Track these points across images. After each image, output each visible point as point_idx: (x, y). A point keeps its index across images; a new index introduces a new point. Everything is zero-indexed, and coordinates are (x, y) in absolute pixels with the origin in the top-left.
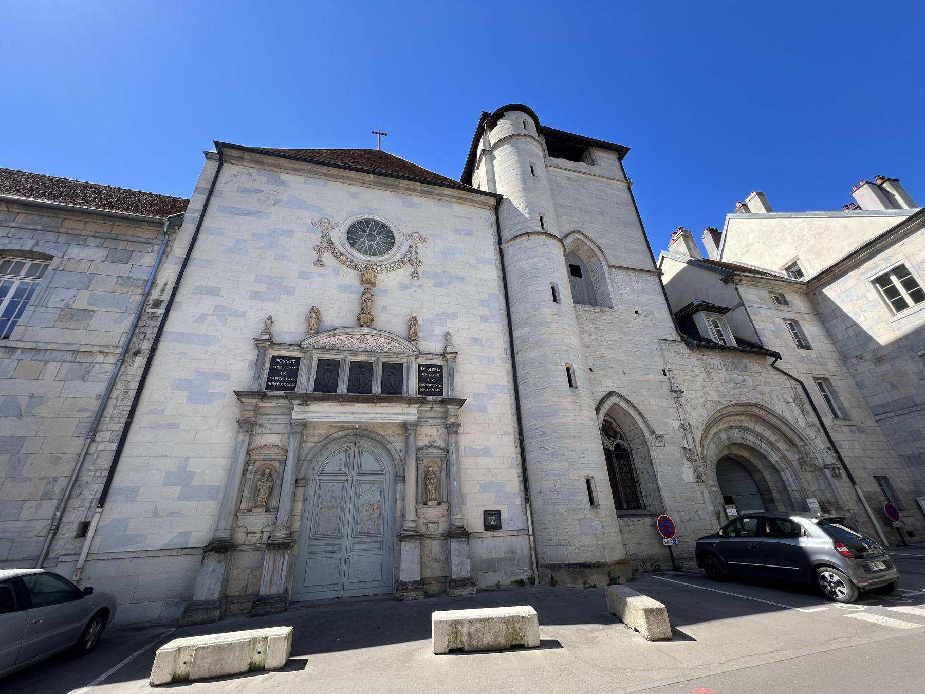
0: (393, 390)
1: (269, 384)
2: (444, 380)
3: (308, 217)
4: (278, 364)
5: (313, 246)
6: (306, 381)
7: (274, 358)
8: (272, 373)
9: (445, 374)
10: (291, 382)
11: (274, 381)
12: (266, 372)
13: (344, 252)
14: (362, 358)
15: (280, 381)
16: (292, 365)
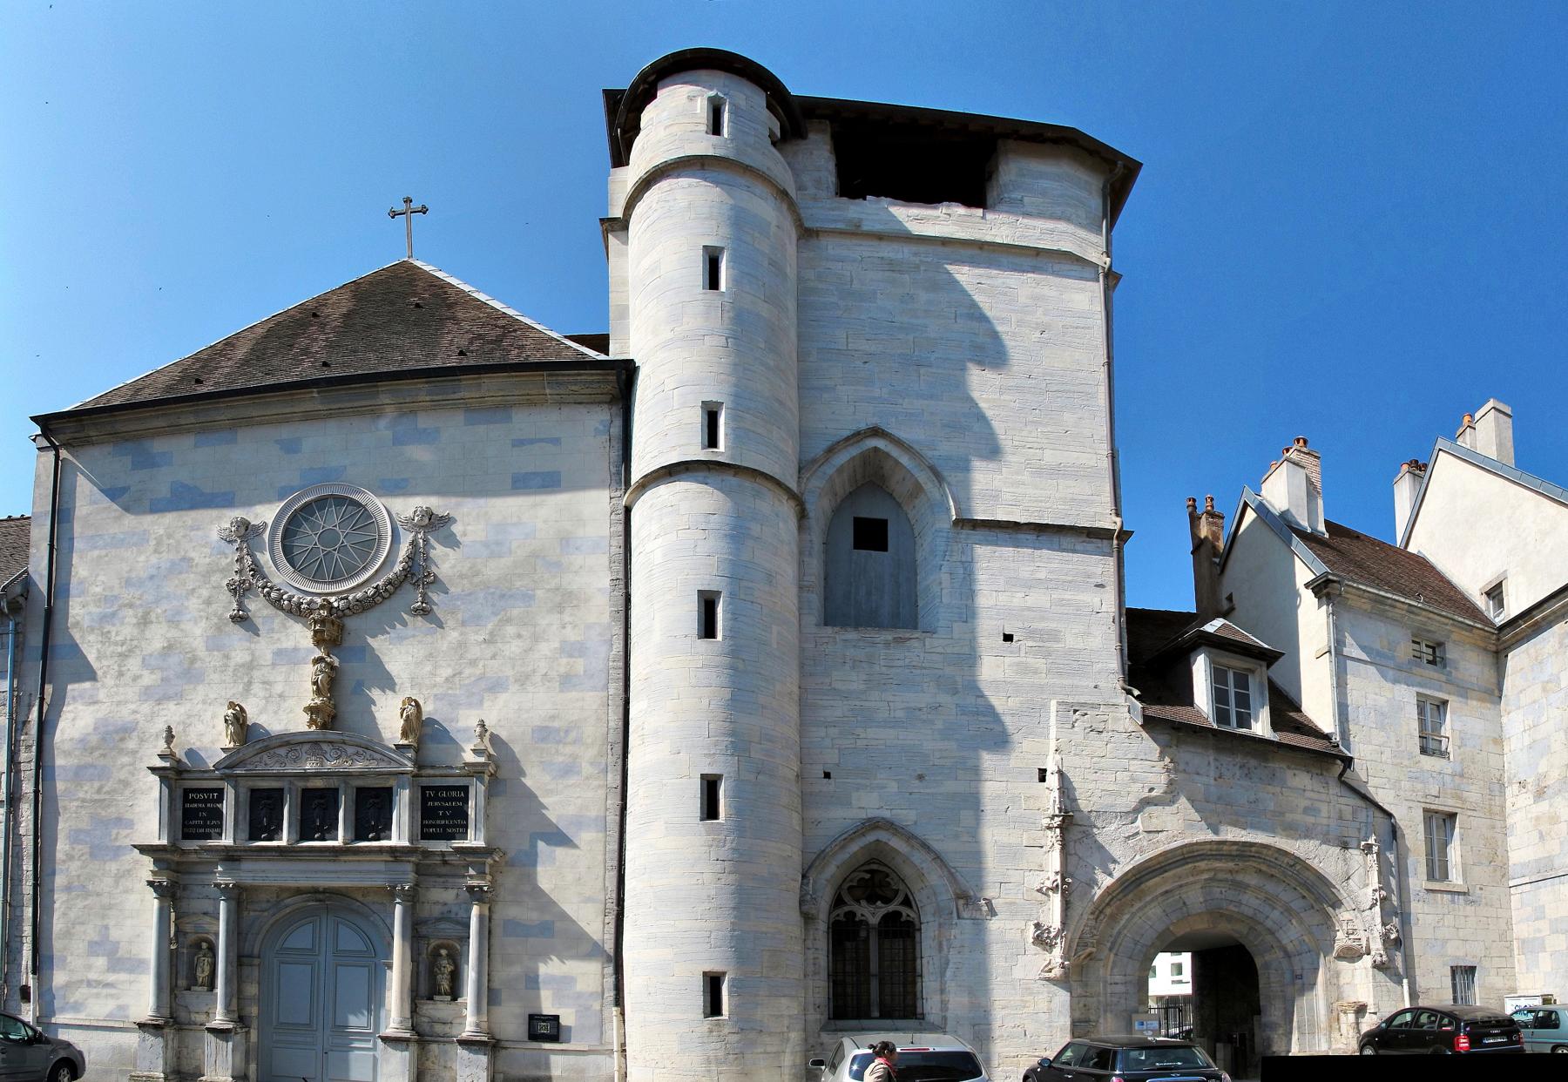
4: (193, 801)
7: (187, 792)
8: (188, 815)
12: (180, 813)
14: (318, 783)
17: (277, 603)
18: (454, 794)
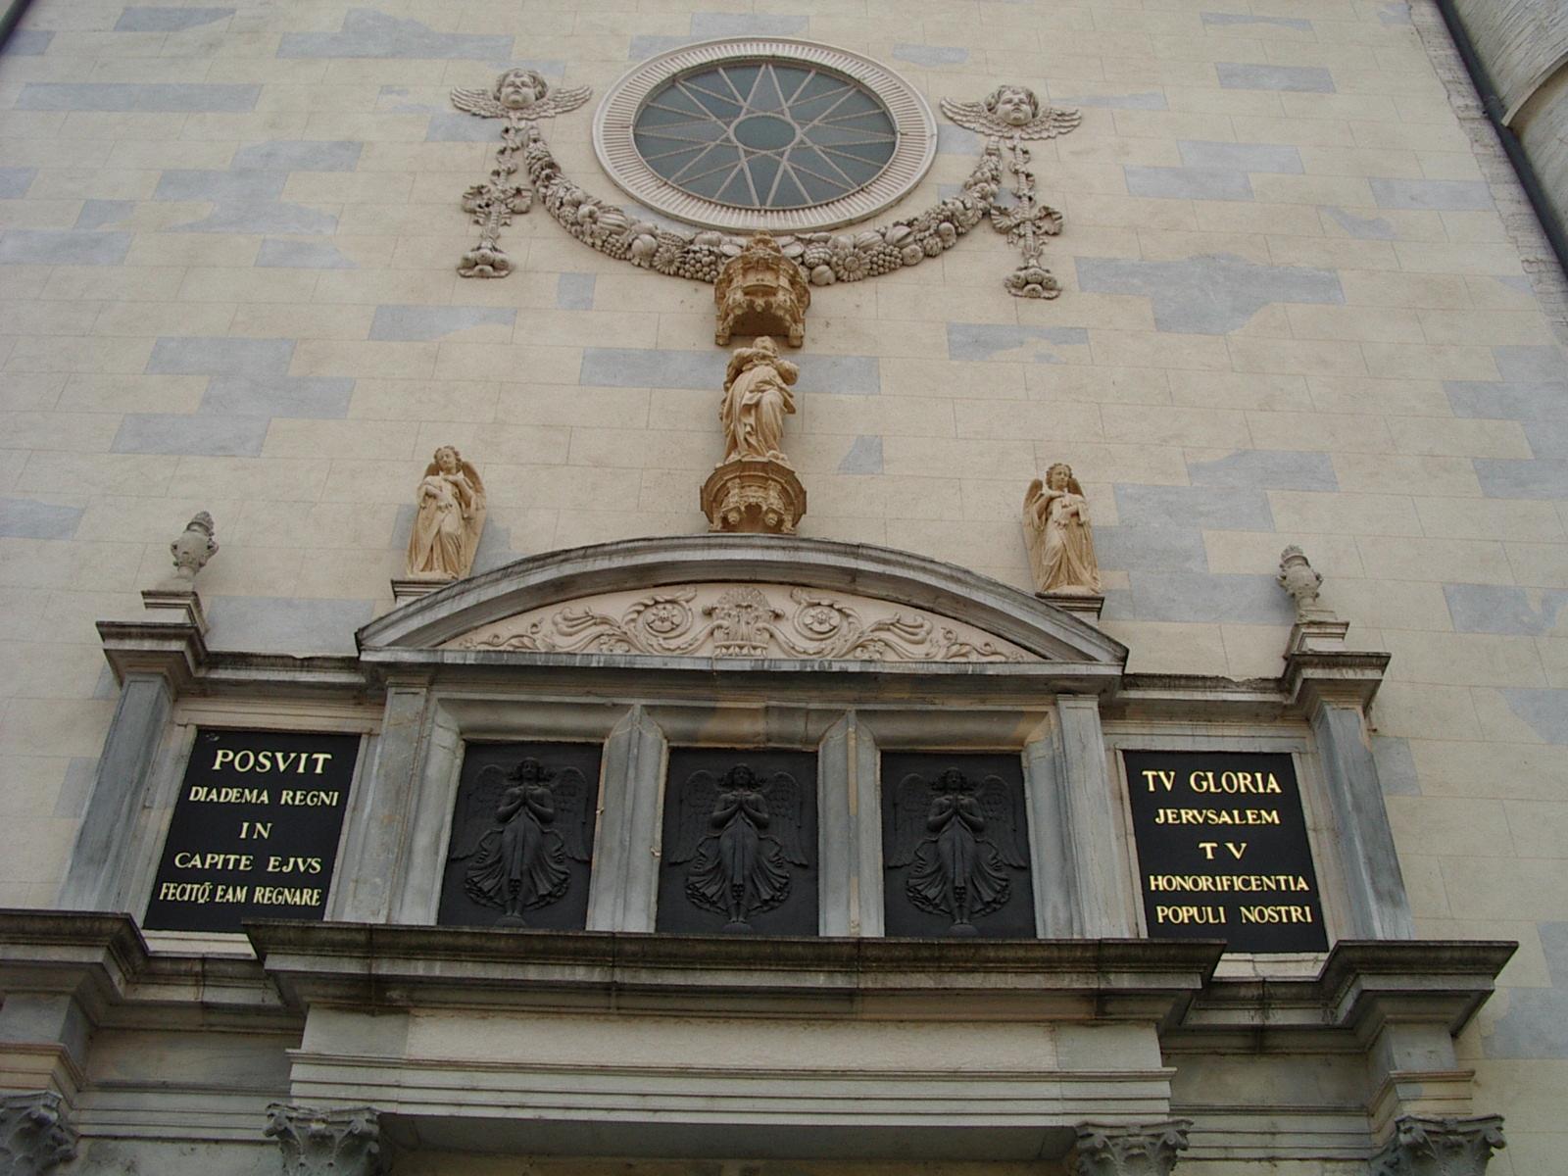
0: (966, 914)
1: (170, 891)
2: (1320, 845)
3: (434, 84)
4: (228, 777)
5: (456, 196)
6: (389, 871)
7: (208, 739)
8: (192, 827)
9: (1314, 809)
10: (297, 881)
11: (197, 876)
12: (158, 821)
13: (611, 199)
14: (744, 723)
15: (233, 878)
16: (309, 782)
17: (615, 247)
18: (1242, 781)
